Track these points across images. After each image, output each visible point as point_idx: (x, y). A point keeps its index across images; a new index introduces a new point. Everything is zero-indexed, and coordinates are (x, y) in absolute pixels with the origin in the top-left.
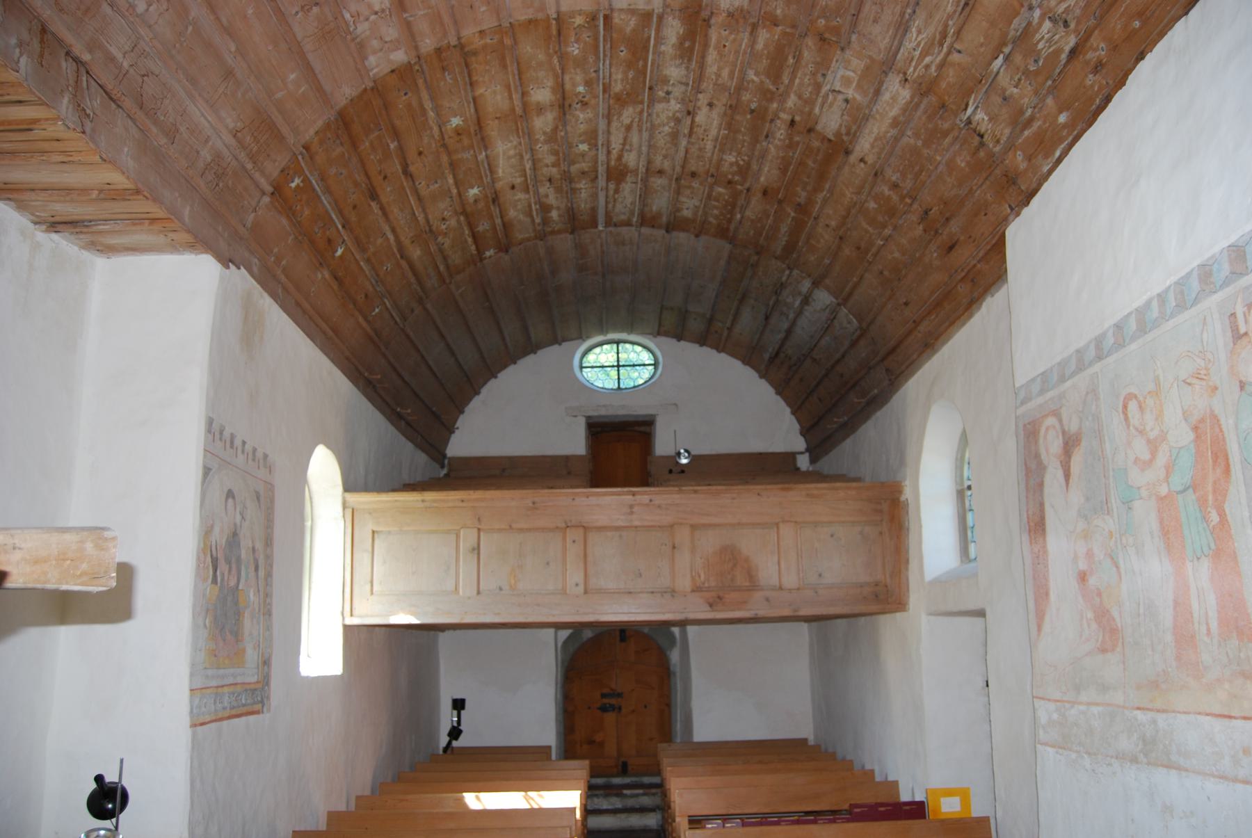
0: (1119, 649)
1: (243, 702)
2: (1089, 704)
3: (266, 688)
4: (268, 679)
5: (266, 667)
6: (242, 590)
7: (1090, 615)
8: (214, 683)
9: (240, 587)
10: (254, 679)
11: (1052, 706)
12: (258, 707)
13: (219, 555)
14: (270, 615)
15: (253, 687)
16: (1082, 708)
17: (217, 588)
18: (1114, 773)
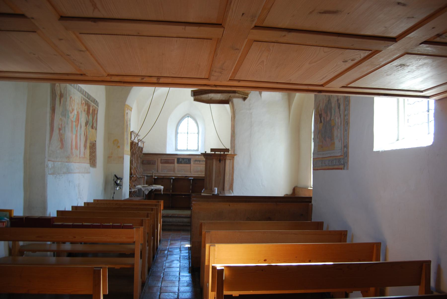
0: (63, 149)
1: (334, 164)
2: (58, 162)
3: (346, 158)
4: (347, 154)
5: (345, 149)
6: (333, 119)
7: (60, 139)
8: (321, 156)
9: (332, 119)
10: (340, 154)
11: (52, 163)
12: (341, 166)
13: (322, 112)
14: (347, 124)
15: (339, 158)
16: (57, 163)
17: (322, 124)
18: (63, 177)
